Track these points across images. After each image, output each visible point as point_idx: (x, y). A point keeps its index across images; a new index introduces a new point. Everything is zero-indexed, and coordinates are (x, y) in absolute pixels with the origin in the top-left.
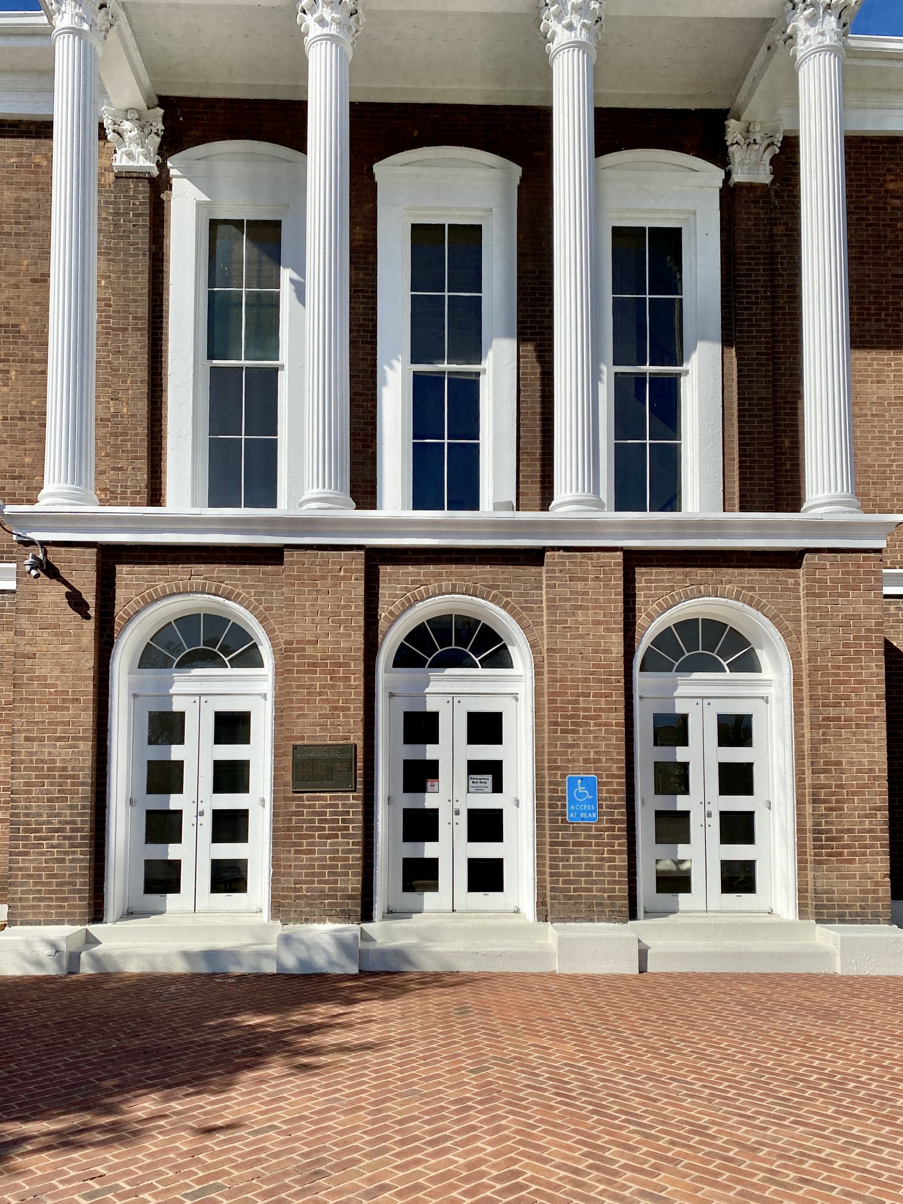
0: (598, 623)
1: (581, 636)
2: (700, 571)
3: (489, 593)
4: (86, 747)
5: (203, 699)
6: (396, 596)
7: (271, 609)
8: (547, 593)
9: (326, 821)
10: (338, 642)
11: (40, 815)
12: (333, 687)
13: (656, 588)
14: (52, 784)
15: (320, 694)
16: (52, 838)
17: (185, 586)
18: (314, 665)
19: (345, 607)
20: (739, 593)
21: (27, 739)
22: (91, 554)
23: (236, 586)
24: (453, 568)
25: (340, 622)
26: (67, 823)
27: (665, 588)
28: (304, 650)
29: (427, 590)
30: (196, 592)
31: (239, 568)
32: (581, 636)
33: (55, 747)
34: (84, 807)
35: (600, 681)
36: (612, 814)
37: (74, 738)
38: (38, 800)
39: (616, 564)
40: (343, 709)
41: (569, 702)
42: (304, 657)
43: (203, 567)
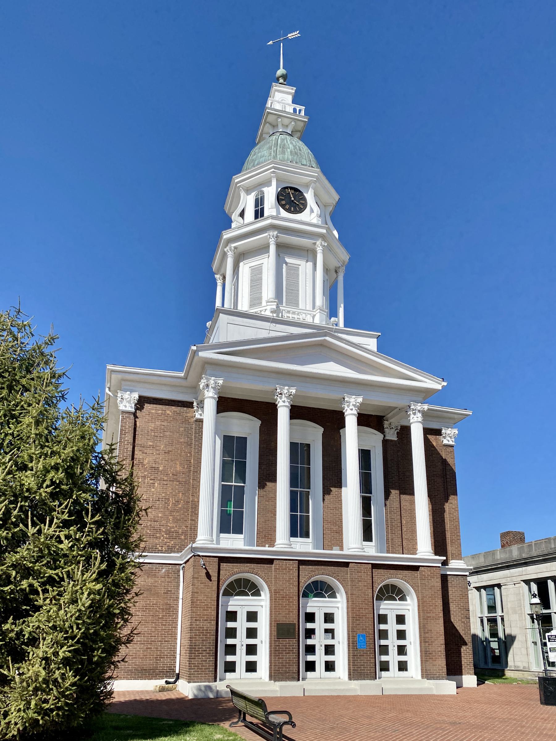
0: (365, 586)
1: (360, 590)
2: (392, 571)
3: (333, 575)
4: (214, 623)
5: (243, 607)
6: (306, 575)
7: (269, 578)
8: (350, 576)
9: (287, 648)
10: (290, 590)
11: (199, 646)
12: (288, 604)
13: (380, 575)
14: (203, 635)
15: (285, 607)
16: (203, 653)
17: (243, 570)
18: (283, 597)
19: (292, 579)
20: (402, 578)
21: (196, 620)
22: (216, 560)
23: (259, 571)
24: (323, 567)
25: (291, 583)
26: (208, 648)
27: (383, 575)
28: (280, 592)
29: (315, 574)
30: (247, 572)
31: (259, 565)
32: (360, 590)
33: (204, 623)
34: (213, 643)
35: (366, 604)
36: (370, 646)
37: (210, 620)
38: (199, 640)
39: (370, 568)
40: (292, 612)
41: (357, 611)
42: (281, 595)
43: (248, 564)
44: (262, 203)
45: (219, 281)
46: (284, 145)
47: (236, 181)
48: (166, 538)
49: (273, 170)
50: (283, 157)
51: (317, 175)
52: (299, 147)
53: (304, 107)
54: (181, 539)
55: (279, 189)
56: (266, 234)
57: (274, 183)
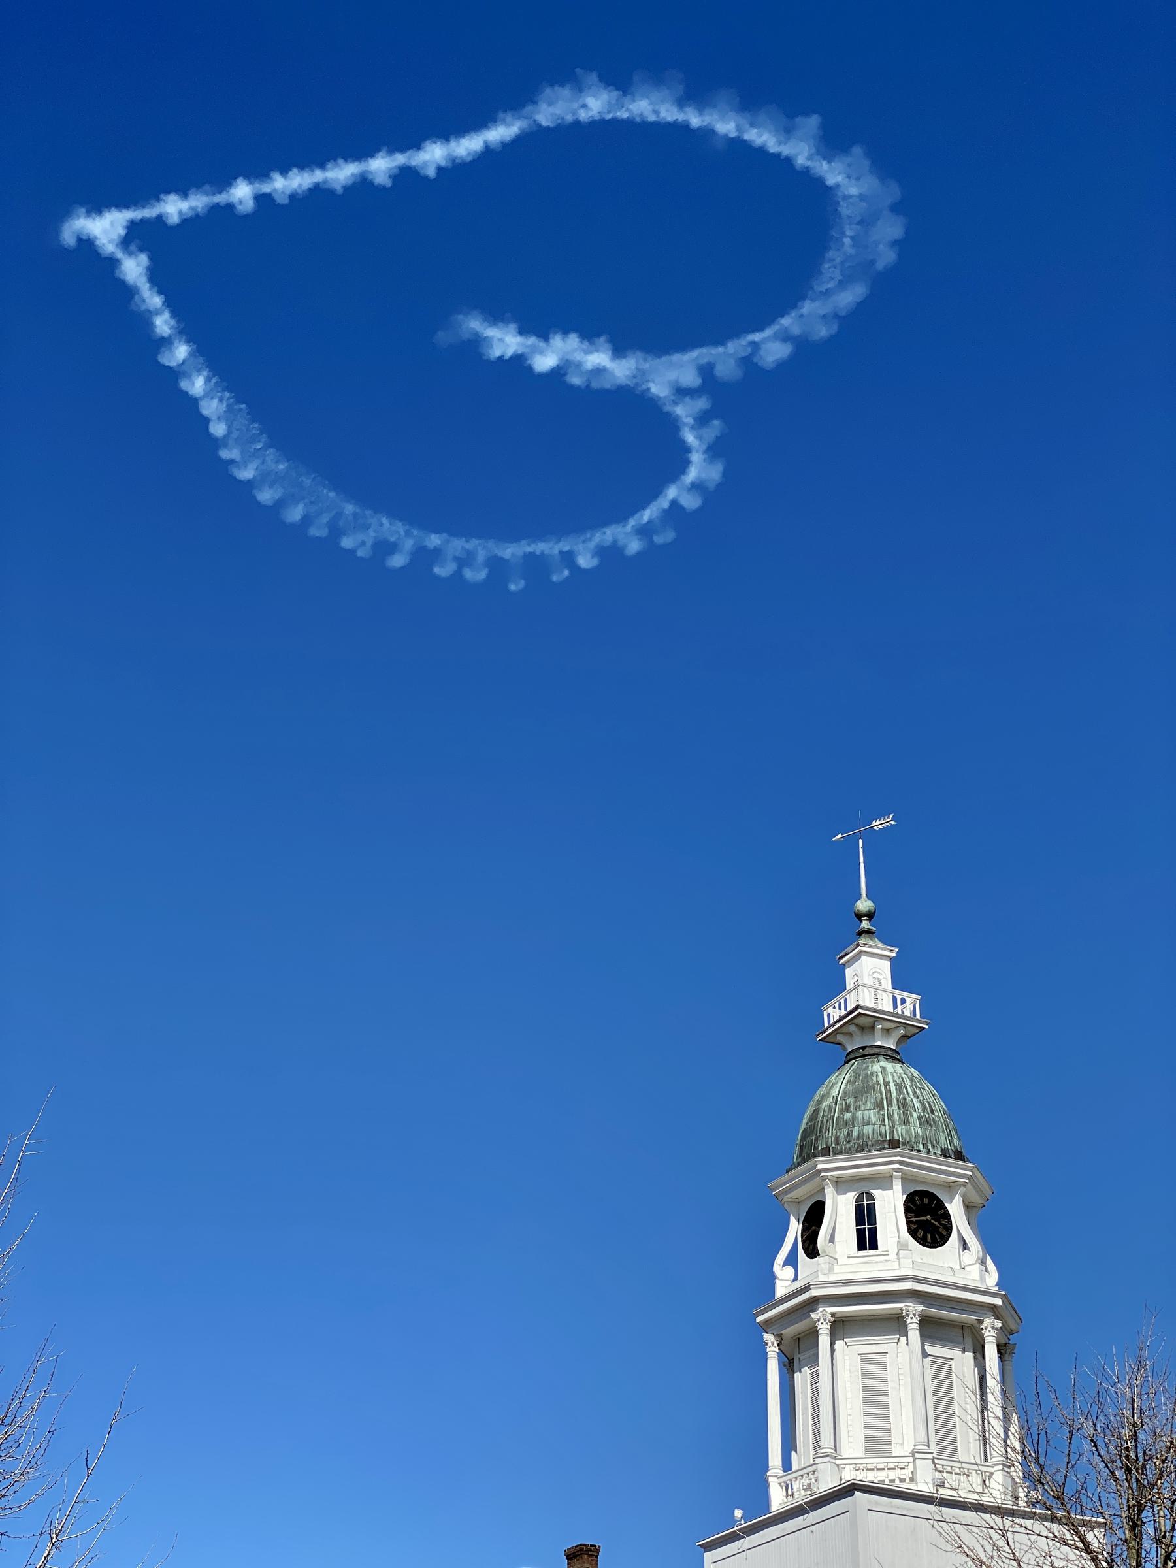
44: (872, 1219)
46: (905, 1099)
47: (819, 1167)
49: (897, 1166)
50: (907, 1131)
51: (971, 1173)
52: (929, 1103)
53: (919, 997)
55: (905, 1196)
57: (897, 1185)
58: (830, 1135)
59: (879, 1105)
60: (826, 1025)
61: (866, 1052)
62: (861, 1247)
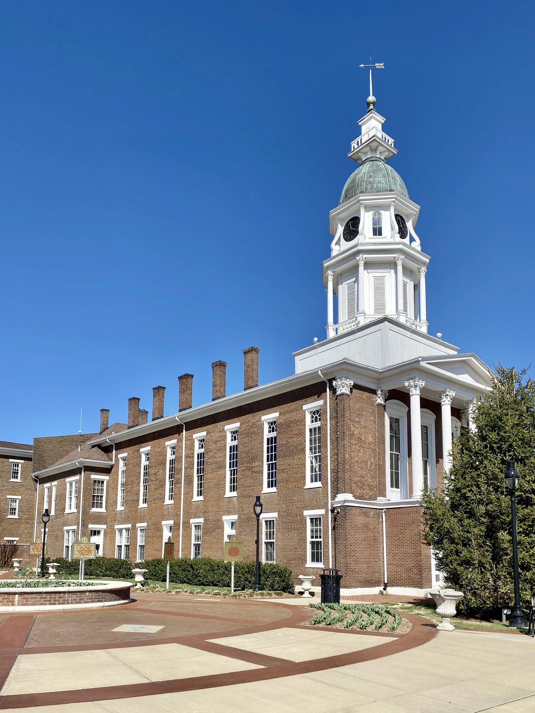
45: (331, 277)
48: (368, 490)
49: (394, 200)
54: (375, 491)
56: (397, 255)
57: (392, 210)
58: (363, 187)
59: (384, 176)
60: (352, 150)
61: (374, 159)
62: (375, 234)
